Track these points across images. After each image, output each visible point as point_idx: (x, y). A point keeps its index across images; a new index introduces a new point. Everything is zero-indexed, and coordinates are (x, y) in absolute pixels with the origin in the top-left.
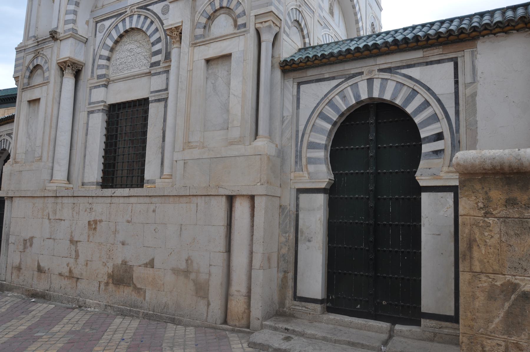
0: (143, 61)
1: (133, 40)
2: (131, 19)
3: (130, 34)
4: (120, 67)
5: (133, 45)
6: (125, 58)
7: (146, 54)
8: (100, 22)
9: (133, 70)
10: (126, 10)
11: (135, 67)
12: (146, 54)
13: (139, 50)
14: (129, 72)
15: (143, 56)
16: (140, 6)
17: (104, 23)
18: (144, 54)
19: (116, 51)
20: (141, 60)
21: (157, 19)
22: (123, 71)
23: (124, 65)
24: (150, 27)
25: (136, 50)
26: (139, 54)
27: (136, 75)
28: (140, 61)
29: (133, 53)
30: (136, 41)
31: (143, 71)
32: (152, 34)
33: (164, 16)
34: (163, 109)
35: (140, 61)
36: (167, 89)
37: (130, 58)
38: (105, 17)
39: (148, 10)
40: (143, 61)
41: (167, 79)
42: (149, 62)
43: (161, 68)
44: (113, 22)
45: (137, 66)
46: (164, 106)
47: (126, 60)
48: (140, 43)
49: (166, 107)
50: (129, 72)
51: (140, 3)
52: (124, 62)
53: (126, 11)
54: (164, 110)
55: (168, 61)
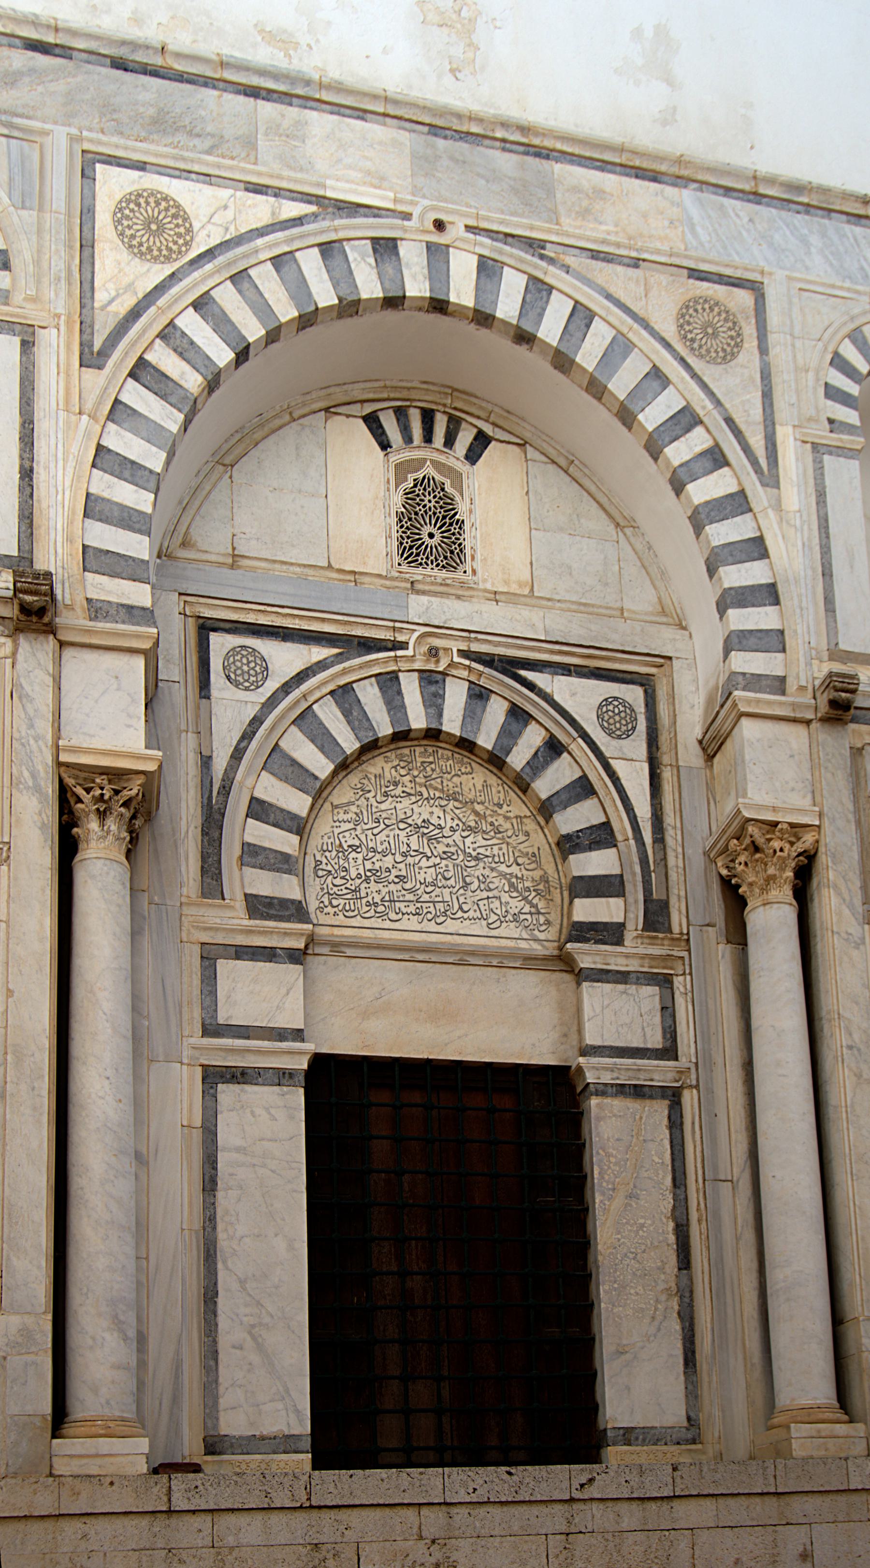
0: (505, 897)
1: (436, 789)
2: (433, 688)
3: (419, 754)
4: (374, 891)
5: (438, 812)
6: (399, 858)
7: (515, 869)
8: (228, 631)
9: (451, 926)
10: (401, 638)
11: (460, 914)
12: (515, 869)
13: (473, 843)
14: (432, 927)
15: (503, 875)
16: (475, 647)
17: (265, 646)
18: (503, 868)
19: (335, 807)
20: (495, 893)
21: (580, 740)
22: (393, 916)
23: (392, 887)
24: (546, 764)
25: (457, 837)
26: (477, 859)
27: (472, 953)
28: (485, 894)
29: (441, 848)
30: (456, 800)
31: (511, 944)
32: (564, 797)
33: (615, 743)
34: (667, 1132)
35: (485, 894)
36: (669, 1052)
37: (424, 863)
38: (263, 620)
39: (531, 686)
40: (505, 897)
41: (668, 1010)
42: (539, 913)
43: (627, 956)
44: (321, 666)
45: (471, 914)
46: (665, 1121)
47: (402, 866)
48: (477, 814)
49: (675, 1124)
50: (432, 927)
51: (480, 636)
52: (394, 872)
53: (404, 646)
54: (671, 1135)
55: (661, 935)
